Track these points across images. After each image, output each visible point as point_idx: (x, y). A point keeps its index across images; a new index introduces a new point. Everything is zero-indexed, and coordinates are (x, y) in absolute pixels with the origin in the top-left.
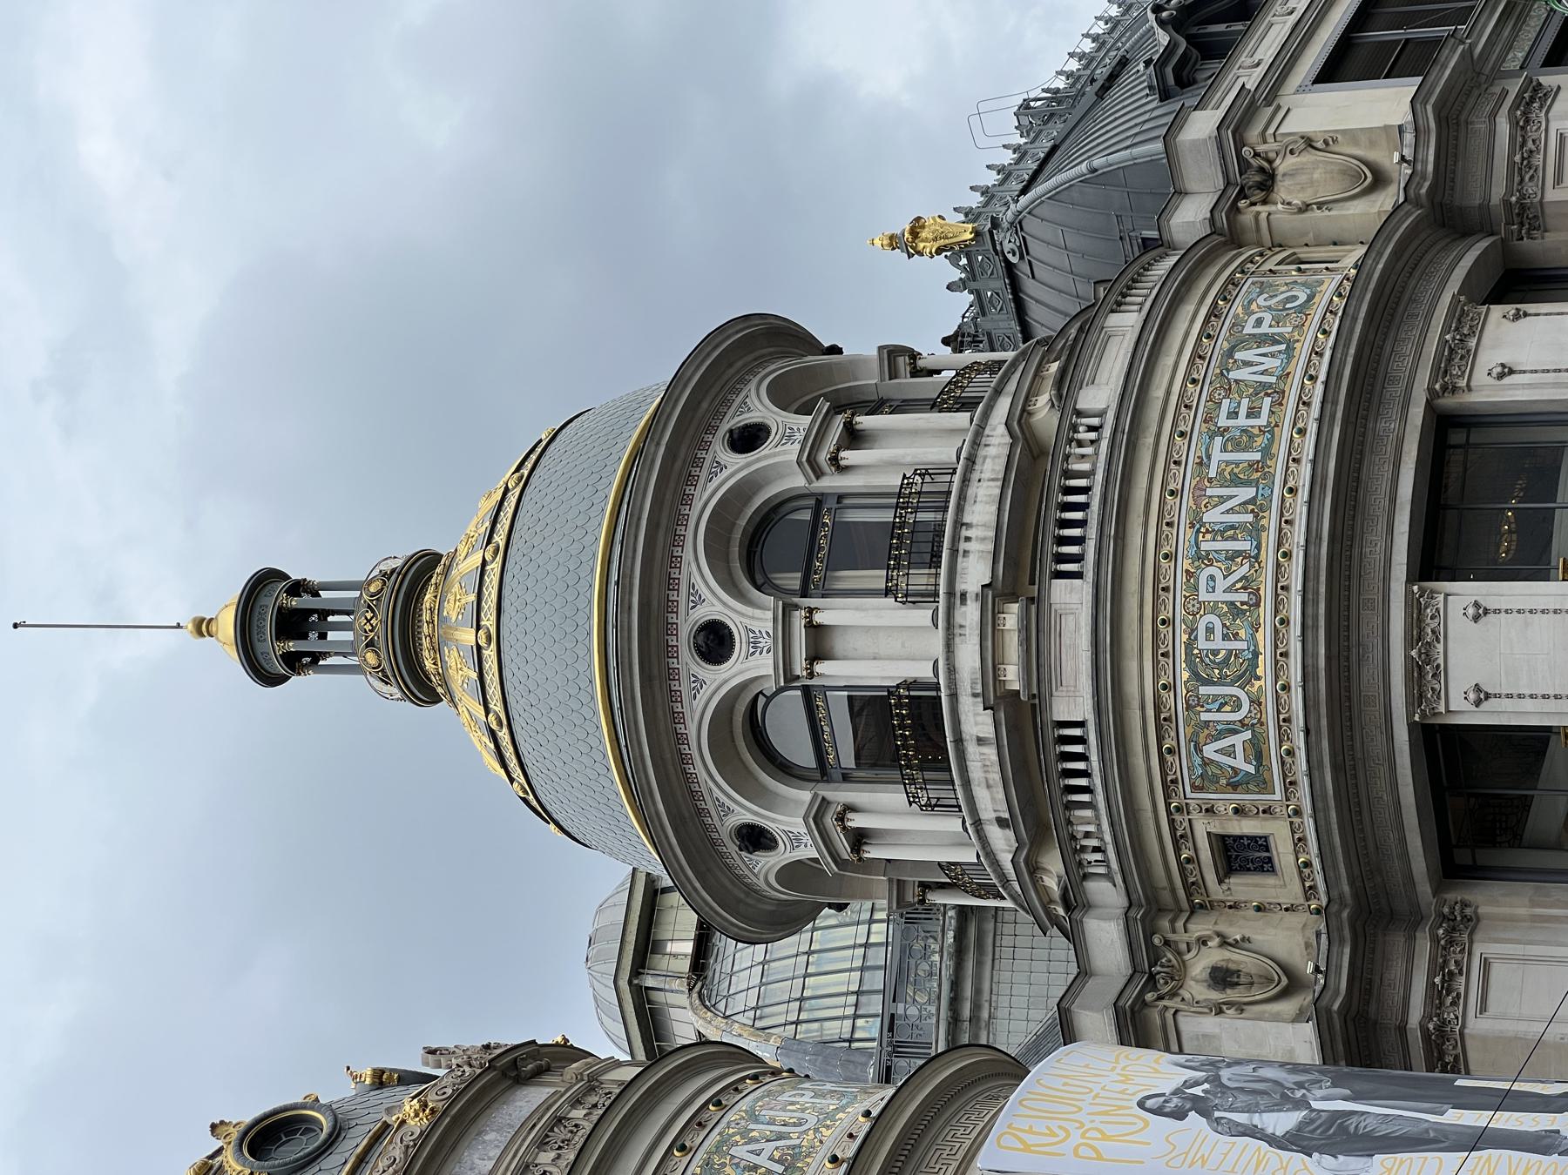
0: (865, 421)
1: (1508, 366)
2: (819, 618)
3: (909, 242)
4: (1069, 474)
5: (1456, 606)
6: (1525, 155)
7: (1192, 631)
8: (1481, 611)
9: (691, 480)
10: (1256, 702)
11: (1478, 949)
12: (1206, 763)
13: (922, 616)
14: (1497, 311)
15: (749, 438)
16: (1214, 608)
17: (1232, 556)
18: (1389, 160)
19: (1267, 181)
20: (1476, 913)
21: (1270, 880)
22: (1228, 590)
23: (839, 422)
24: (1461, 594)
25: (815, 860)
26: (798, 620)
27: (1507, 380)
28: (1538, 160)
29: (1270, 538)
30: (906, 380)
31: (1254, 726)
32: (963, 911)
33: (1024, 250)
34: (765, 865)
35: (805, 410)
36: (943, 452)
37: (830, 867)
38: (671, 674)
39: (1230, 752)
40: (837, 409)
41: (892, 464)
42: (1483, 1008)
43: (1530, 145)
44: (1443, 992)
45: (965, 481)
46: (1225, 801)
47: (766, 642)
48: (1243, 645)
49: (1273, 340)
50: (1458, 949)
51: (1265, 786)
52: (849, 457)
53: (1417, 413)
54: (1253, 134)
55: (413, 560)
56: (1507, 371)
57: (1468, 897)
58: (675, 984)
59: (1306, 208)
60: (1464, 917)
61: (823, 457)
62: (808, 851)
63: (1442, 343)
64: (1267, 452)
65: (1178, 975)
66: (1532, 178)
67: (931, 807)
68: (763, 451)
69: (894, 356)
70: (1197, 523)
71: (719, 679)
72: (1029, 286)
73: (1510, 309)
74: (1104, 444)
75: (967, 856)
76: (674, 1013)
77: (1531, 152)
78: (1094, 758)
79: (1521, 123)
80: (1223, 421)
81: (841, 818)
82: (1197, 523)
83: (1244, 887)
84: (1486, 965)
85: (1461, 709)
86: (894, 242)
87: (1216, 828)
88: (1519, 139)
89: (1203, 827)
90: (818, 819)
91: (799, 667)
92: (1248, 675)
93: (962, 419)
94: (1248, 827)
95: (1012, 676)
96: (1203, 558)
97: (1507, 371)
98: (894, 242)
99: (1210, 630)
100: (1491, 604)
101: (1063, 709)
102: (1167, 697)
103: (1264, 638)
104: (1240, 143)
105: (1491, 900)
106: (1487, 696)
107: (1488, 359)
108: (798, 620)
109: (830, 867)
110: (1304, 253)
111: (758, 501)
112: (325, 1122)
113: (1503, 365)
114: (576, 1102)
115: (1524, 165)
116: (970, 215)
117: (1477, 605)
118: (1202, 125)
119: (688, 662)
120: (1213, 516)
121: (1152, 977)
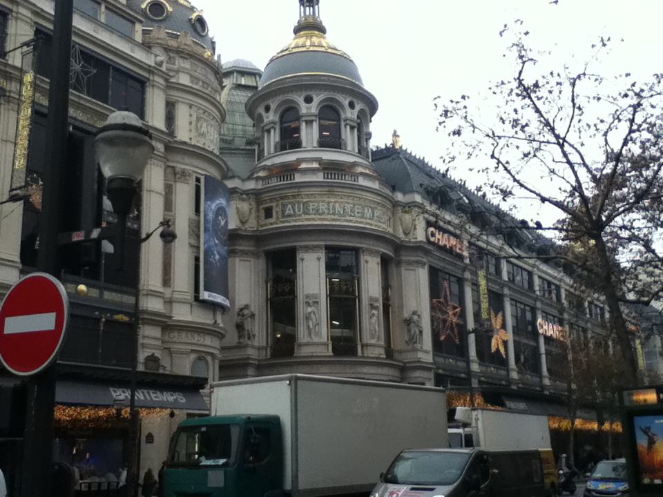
0: (356, 130)
2: (314, 123)
3: (395, 135)
4: (345, 176)
5: (320, 254)
7: (314, 202)
9: (342, 94)
10: (300, 215)
11: (253, 260)
12: (287, 205)
13: (315, 145)
14: (379, 260)
15: (352, 105)
16: (318, 206)
17: (329, 209)
18: (411, 236)
19: (406, 212)
21: (264, 218)
22: (322, 209)
23: (356, 125)
24: (322, 255)
25: (263, 121)
26: (314, 118)
29: (333, 217)
30: (365, 137)
31: (294, 215)
32: (254, 150)
33: (393, 159)
34: (261, 110)
35: (358, 117)
36: (349, 148)
37: (262, 125)
38: (301, 90)
39: (289, 210)
40: (358, 124)
41: (346, 137)
42: (240, 260)
44: (244, 253)
45: (344, 153)
46: (279, 209)
47: (309, 111)
48: (311, 212)
49: (373, 214)
51: (284, 216)
52: (348, 127)
53: (358, 245)
54: (416, 209)
55: (324, 28)
58: (235, 80)
59: (401, 220)
61: (348, 122)
62: (266, 120)
63: (373, 250)
64: (351, 216)
65: (243, 200)
67: (276, 147)
68: (349, 109)
69: (369, 135)
70: (336, 202)
71: (300, 100)
72: (386, 160)
73: (380, 262)
74: (350, 182)
75: (266, 154)
76: (229, 80)
78: (288, 182)
80: (356, 207)
81: (273, 127)
82: (336, 202)
83: (262, 213)
84: (249, 261)
85: (300, 255)
86: (395, 132)
87: (274, 207)
89: (274, 204)
90: (272, 123)
91: (304, 119)
92: (306, 213)
93: (357, 151)
94: (274, 214)
95: (303, 166)
96: (329, 203)
97: (367, 262)
98: (395, 132)
99: (314, 205)
100: (321, 262)
101: (297, 175)
102: (300, 197)
103: (313, 216)
104: (415, 206)
105: (261, 263)
107: (369, 258)
108: (314, 118)
109: (262, 125)
110: (392, 220)
111: (339, 108)
112: (204, 34)
114: (212, 88)
115: (409, 263)
116: (401, 147)
118: (418, 198)
119: (304, 94)
120: (337, 205)
121: (242, 194)
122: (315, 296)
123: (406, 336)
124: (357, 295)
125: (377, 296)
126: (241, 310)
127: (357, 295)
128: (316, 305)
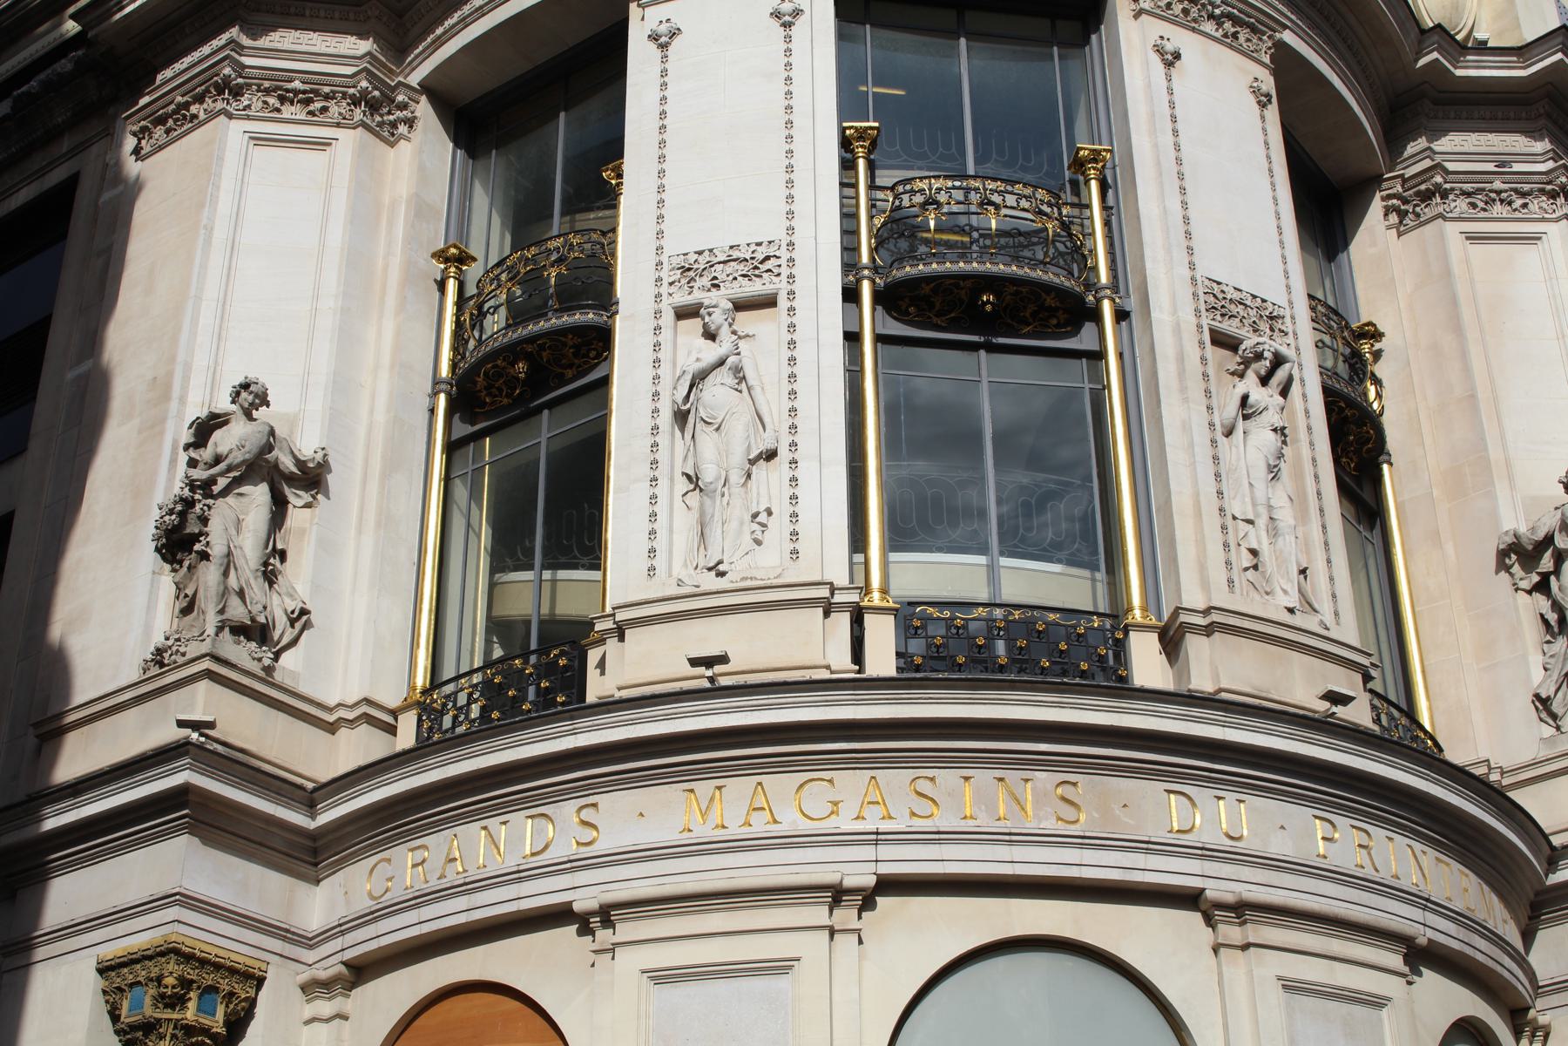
1: (1178, 64)
6: (1504, 195)
8: (787, 18)
11: (348, 141)
20: (402, 137)
27: (1155, 59)
28: (1498, 210)
42: (259, 140)
43: (1518, 202)
44: (282, 91)
50: (344, 111)
56: (1171, 59)
57: (419, 125)
60: (394, 125)
66: (1474, 206)
73: (1268, 84)
77: (1510, 203)
79: (1549, 187)
84: (323, 144)
88: (1526, 187)
97: (1171, 59)
106: (664, 47)
113: (1177, 56)
117: (797, 13)
122: (757, 266)
123: (1536, 661)
124: (1104, 277)
125: (1275, 294)
126: (206, 428)
127: (1104, 277)
128: (745, 320)
